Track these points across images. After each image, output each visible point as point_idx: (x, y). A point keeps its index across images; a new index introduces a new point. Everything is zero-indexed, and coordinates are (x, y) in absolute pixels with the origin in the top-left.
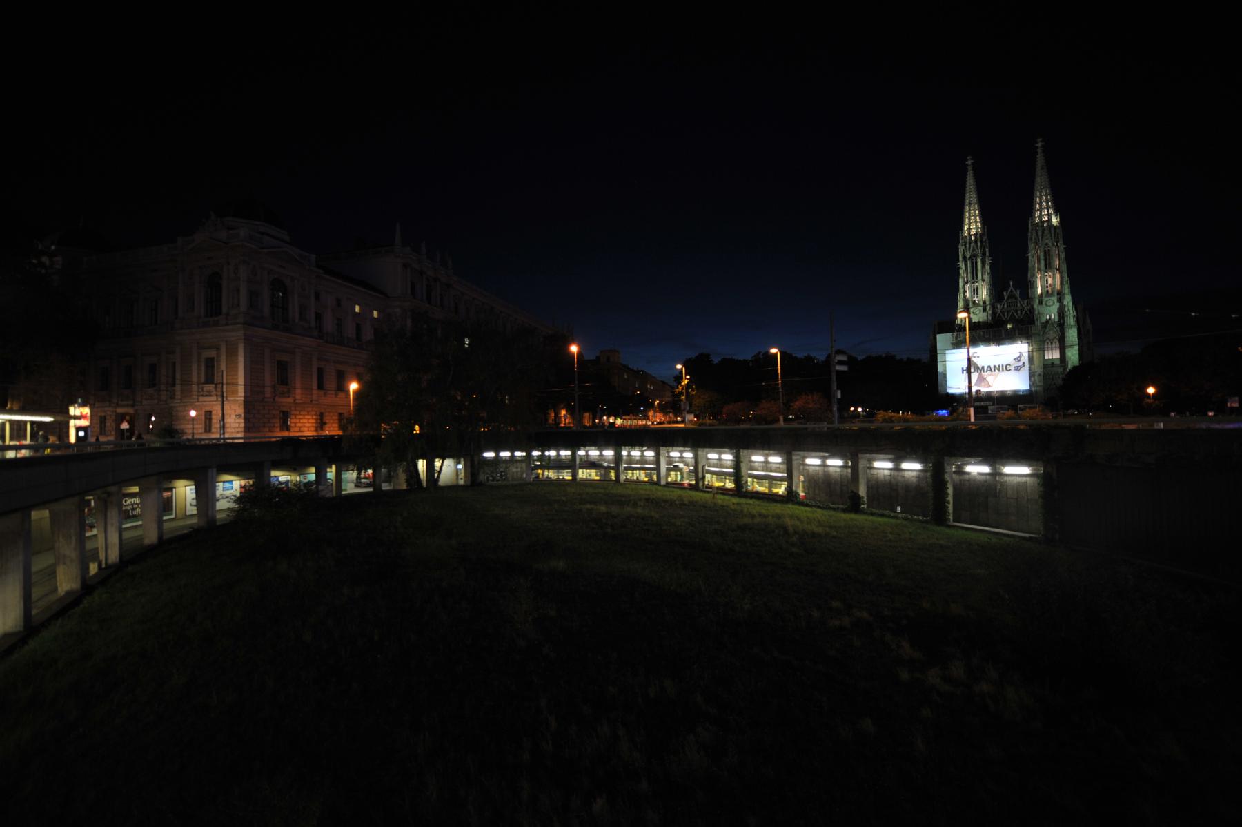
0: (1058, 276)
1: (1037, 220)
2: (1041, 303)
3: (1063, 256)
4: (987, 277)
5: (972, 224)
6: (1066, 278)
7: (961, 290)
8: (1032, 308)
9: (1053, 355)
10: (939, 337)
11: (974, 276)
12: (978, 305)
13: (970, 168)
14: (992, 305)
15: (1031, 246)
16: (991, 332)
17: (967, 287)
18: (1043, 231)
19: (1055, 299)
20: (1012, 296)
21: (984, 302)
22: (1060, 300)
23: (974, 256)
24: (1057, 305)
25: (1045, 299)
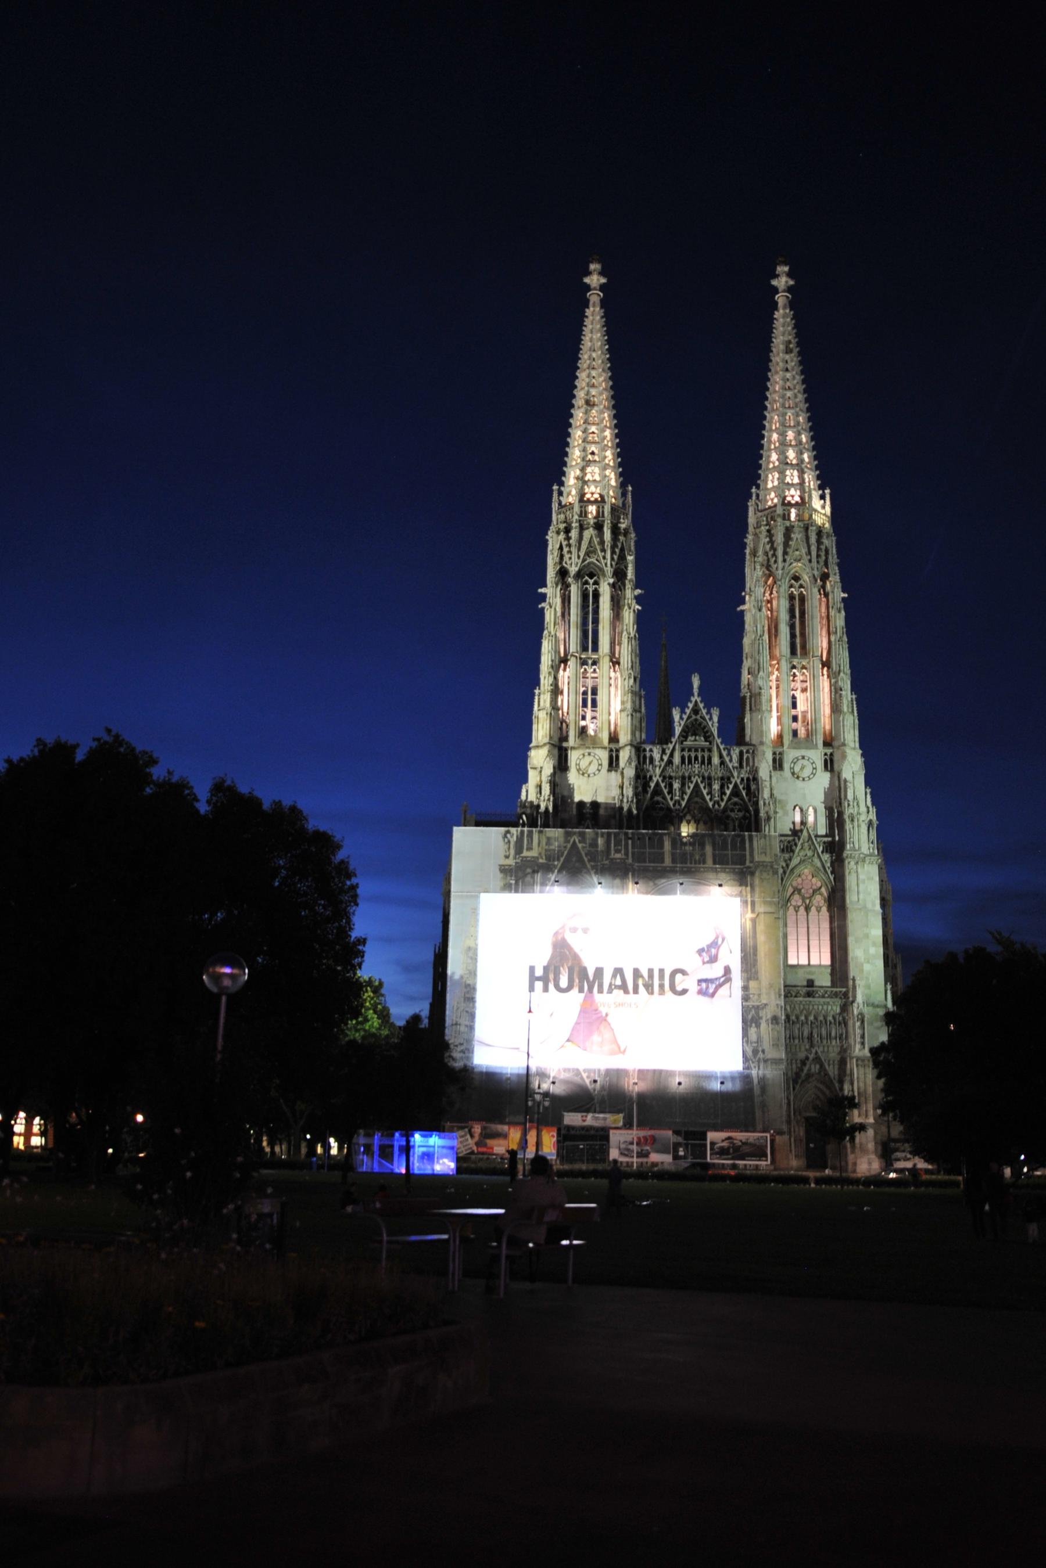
0: (825, 684)
1: (772, 499)
2: (778, 764)
3: (839, 620)
4: (626, 652)
5: (592, 467)
6: (848, 696)
7: (545, 681)
8: (753, 779)
9: (810, 952)
10: (455, 829)
11: (589, 640)
12: (595, 742)
13: (595, 298)
14: (638, 749)
15: (753, 574)
16: (634, 840)
17: (565, 676)
18: (788, 532)
19: (817, 755)
20: (695, 728)
21: (614, 738)
22: (830, 764)
23: (588, 573)
24: (824, 779)
25: (790, 755)
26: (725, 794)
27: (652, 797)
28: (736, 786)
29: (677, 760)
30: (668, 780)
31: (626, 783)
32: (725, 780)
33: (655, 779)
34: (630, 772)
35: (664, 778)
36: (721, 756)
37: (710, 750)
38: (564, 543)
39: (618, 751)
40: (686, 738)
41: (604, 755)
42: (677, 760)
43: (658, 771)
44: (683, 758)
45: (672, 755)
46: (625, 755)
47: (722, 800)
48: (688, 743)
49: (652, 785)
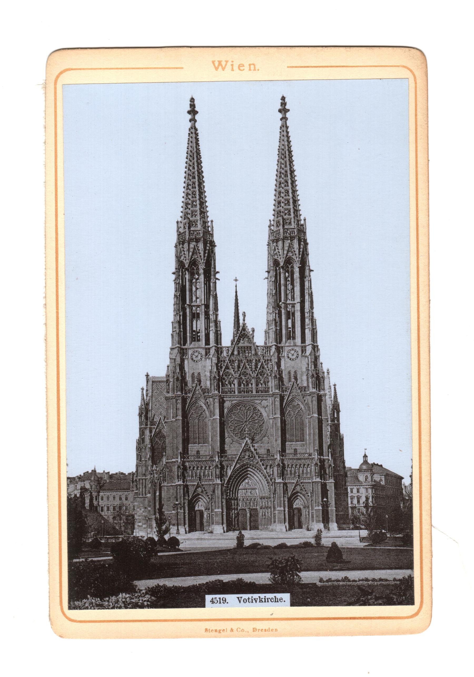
26: (258, 368)
27: (224, 370)
28: (262, 364)
29: (236, 353)
30: (232, 362)
31: (213, 364)
32: (258, 361)
33: (226, 362)
34: (215, 360)
35: (230, 361)
36: (255, 350)
37: (250, 347)
38: (182, 249)
39: (209, 349)
40: (239, 342)
41: (203, 352)
42: (236, 353)
43: (227, 359)
44: (239, 351)
45: (233, 351)
46: (212, 351)
47: (256, 370)
48: (241, 345)
49: (225, 364)
